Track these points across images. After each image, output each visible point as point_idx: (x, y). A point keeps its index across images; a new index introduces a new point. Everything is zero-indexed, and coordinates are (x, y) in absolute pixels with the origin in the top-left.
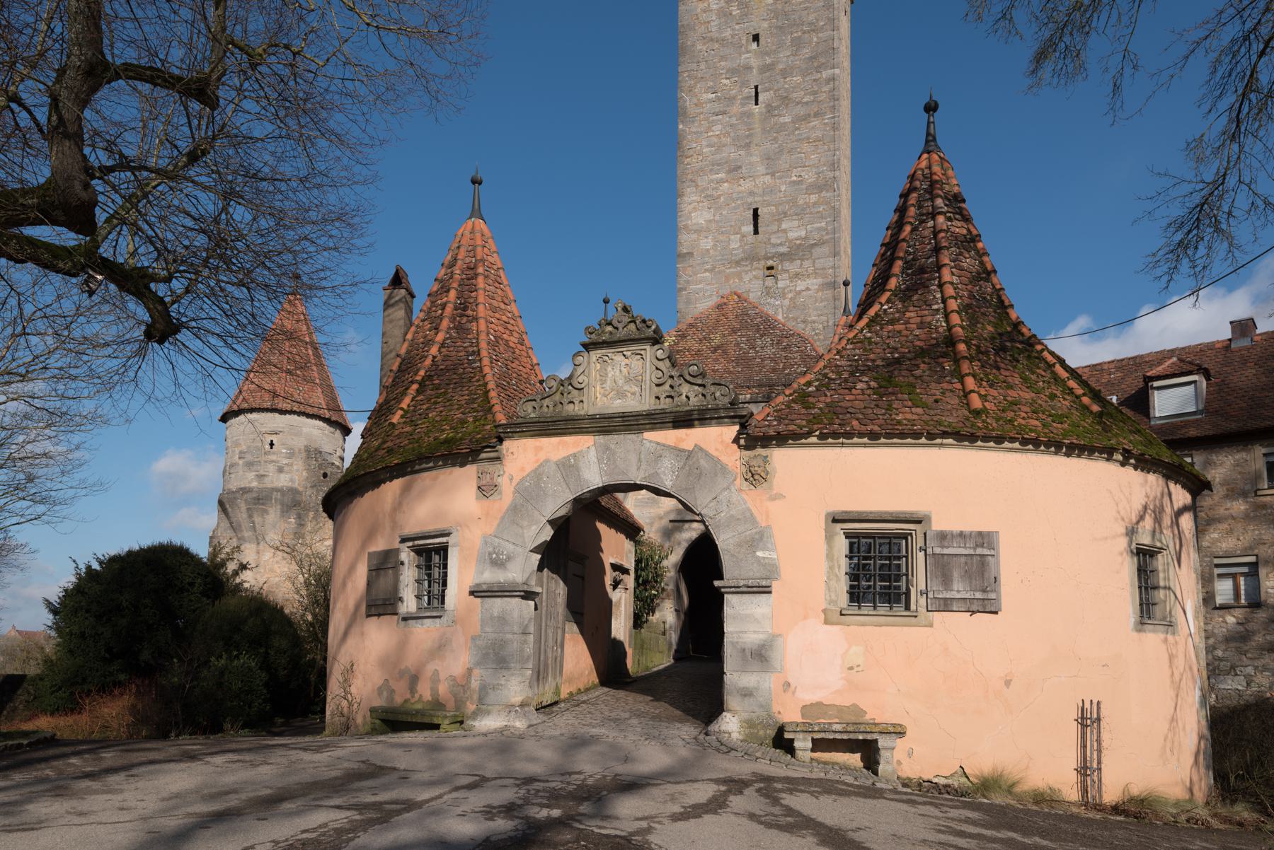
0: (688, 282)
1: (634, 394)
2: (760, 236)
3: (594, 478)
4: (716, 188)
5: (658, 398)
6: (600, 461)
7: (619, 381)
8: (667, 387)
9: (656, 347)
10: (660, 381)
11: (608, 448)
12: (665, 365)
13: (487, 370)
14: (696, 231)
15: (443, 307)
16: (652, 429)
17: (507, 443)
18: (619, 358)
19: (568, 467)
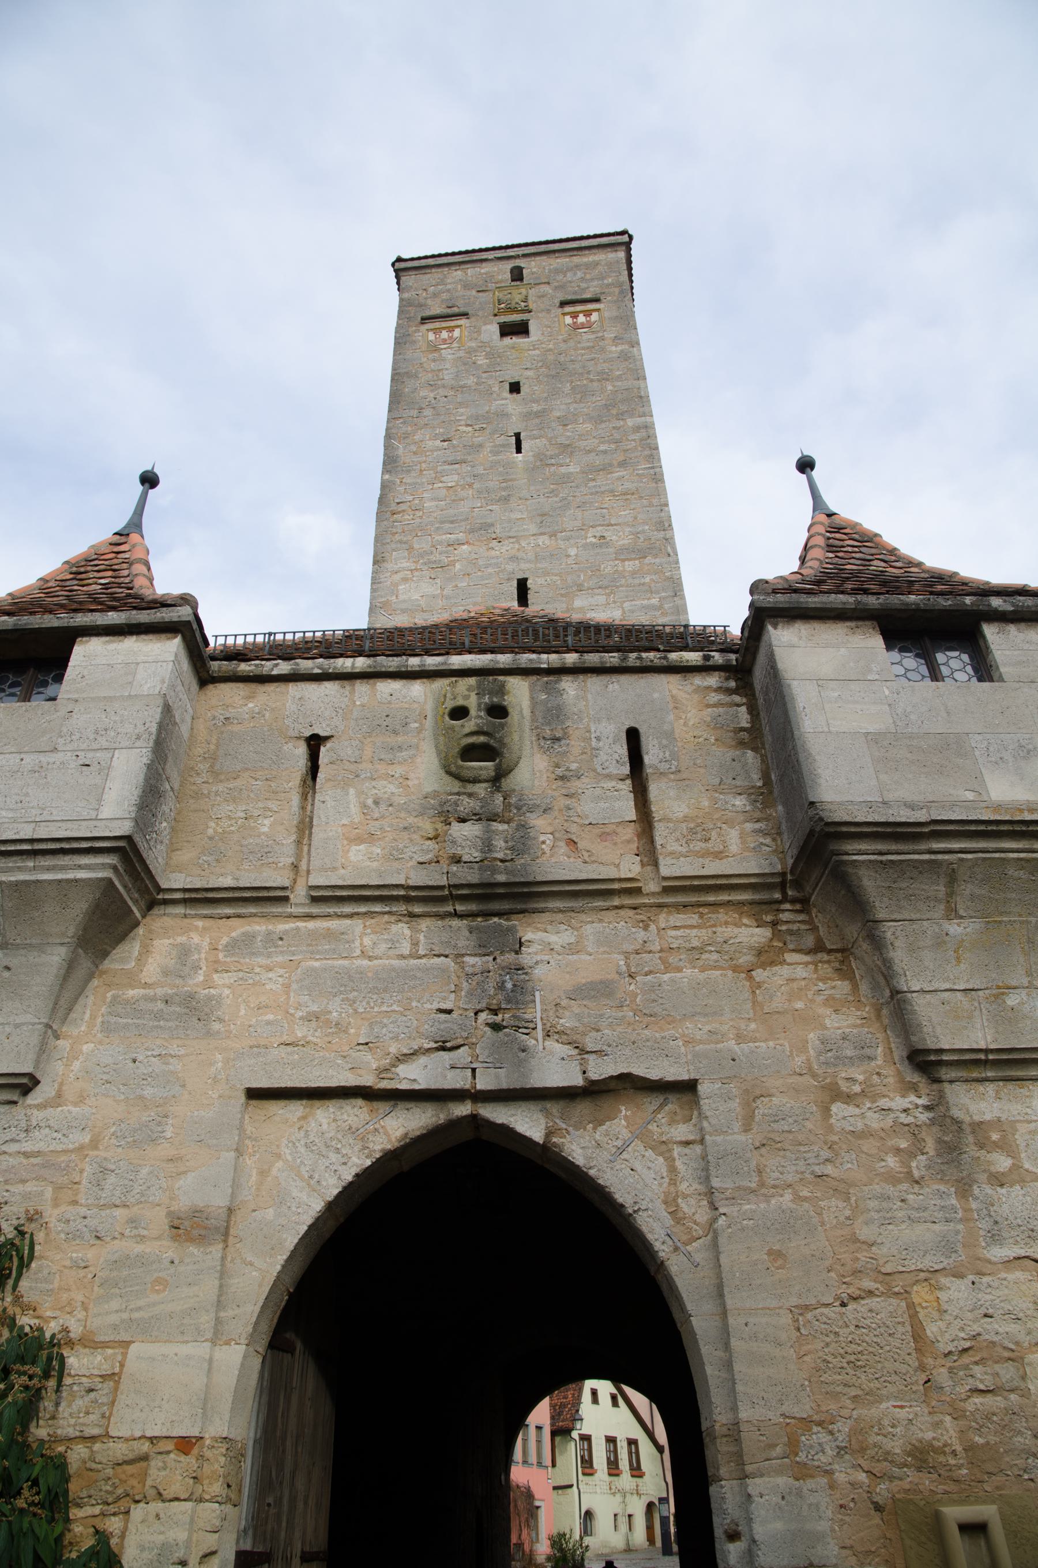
14: (404, 611)
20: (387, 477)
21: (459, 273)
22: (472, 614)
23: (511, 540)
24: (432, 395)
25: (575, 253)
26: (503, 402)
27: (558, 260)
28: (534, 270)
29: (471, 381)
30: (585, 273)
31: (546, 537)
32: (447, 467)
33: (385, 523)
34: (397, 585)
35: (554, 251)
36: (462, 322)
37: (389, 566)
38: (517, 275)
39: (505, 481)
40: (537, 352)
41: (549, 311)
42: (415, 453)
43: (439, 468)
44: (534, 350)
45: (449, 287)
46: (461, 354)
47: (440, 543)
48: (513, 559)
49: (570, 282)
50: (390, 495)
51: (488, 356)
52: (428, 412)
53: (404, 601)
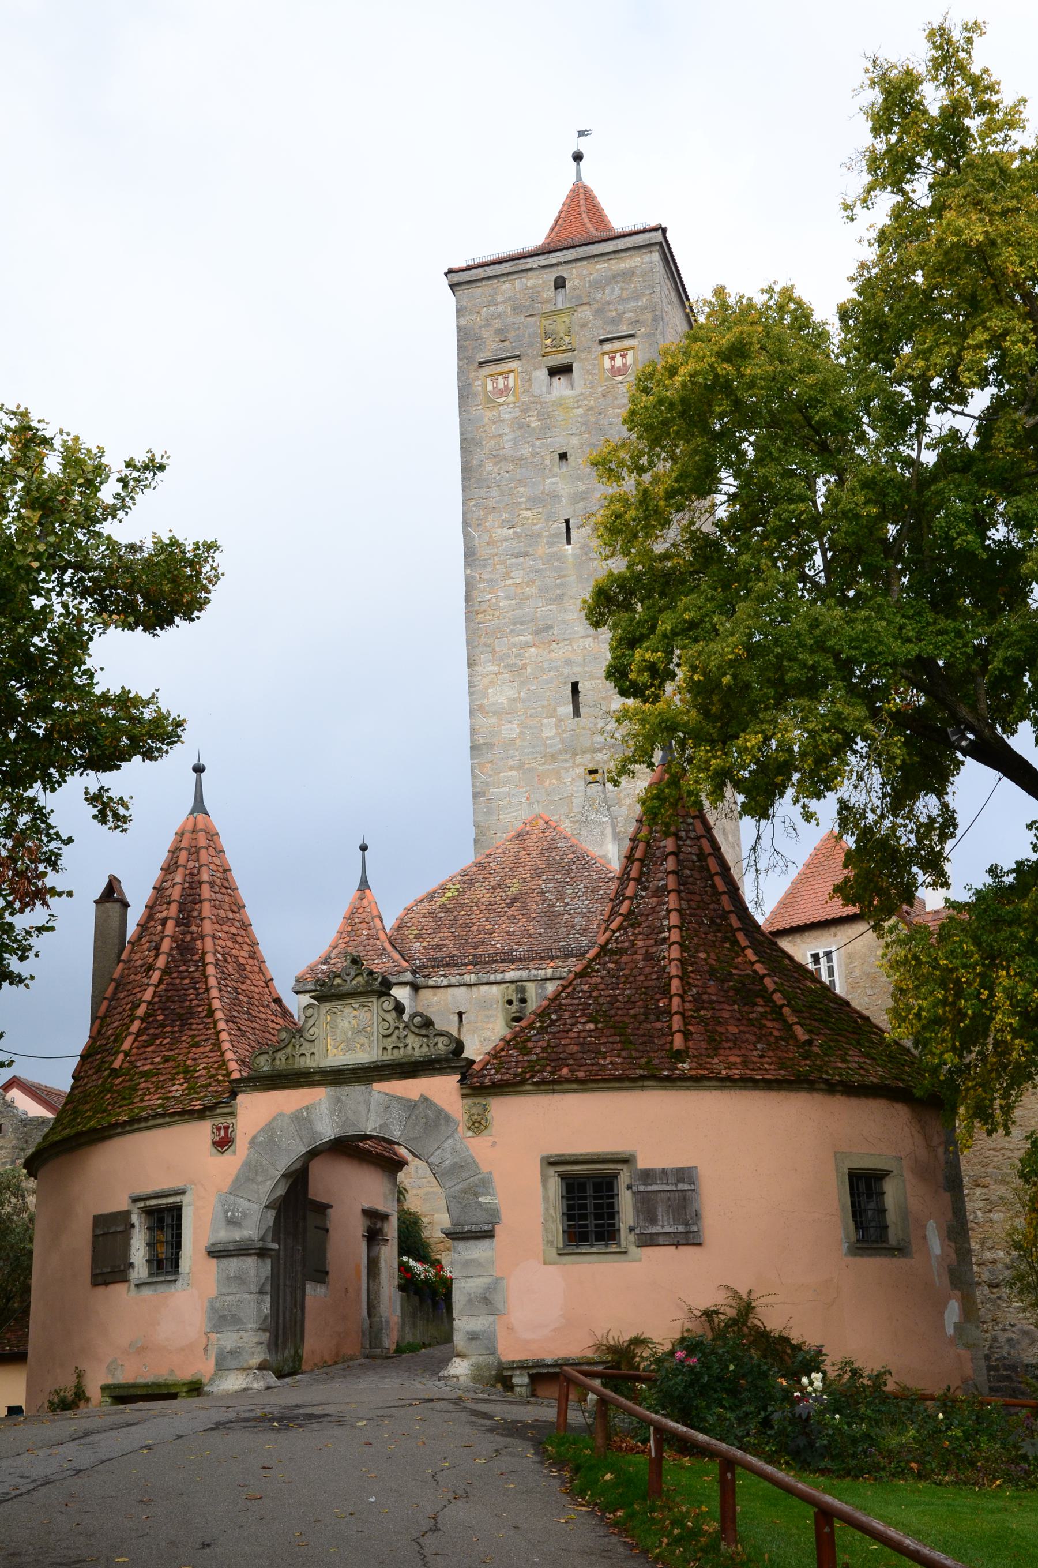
0: (487, 784)
1: (362, 1045)
2: (582, 721)
3: (327, 1130)
4: (520, 655)
5: (385, 1049)
6: (332, 1113)
7: (346, 1036)
8: (394, 1038)
9: (384, 999)
10: (388, 1032)
11: (338, 1100)
12: (391, 1017)
13: (216, 1004)
14: (494, 713)
15: (164, 922)
16: (381, 1080)
17: (240, 1098)
18: (348, 1010)
19: (302, 1119)
20: (469, 572)
21: (507, 285)
22: (528, 828)
23: (567, 642)
24: (496, 470)
25: (613, 256)
26: (554, 480)
27: (598, 267)
28: (576, 283)
29: (526, 451)
30: (622, 289)
31: (590, 639)
32: (513, 560)
33: (472, 624)
34: (486, 688)
35: (593, 256)
36: (514, 365)
37: (478, 668)
38: (560, 284)
39: (561, 577)
40: (580, 411)
41: (589, 349)
42: (488, 544)
43: (509, 562)
44: (578, 408)
45: (500, 308)
46: (517, 413)
47: (514, 645)
48: (568, 662)
49: (609, 303)
50: (475, 593)
51: (541, 416)
52: (494, 492)
53: (493, 704)
